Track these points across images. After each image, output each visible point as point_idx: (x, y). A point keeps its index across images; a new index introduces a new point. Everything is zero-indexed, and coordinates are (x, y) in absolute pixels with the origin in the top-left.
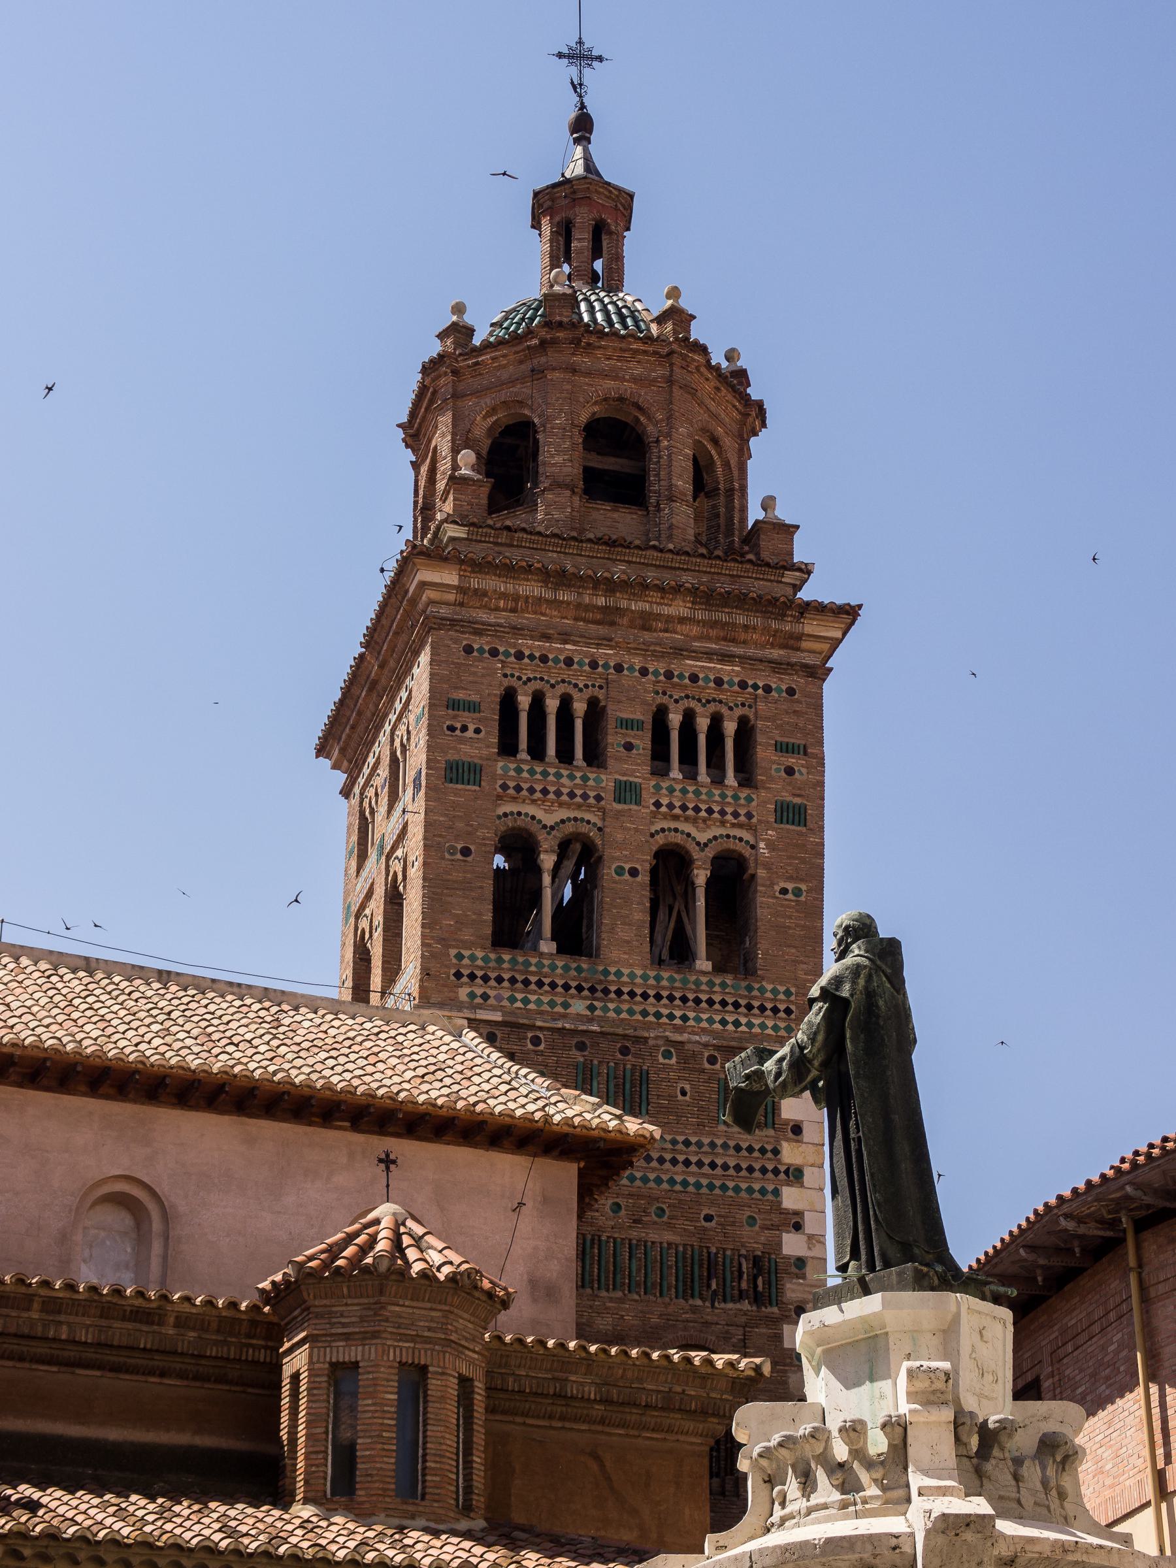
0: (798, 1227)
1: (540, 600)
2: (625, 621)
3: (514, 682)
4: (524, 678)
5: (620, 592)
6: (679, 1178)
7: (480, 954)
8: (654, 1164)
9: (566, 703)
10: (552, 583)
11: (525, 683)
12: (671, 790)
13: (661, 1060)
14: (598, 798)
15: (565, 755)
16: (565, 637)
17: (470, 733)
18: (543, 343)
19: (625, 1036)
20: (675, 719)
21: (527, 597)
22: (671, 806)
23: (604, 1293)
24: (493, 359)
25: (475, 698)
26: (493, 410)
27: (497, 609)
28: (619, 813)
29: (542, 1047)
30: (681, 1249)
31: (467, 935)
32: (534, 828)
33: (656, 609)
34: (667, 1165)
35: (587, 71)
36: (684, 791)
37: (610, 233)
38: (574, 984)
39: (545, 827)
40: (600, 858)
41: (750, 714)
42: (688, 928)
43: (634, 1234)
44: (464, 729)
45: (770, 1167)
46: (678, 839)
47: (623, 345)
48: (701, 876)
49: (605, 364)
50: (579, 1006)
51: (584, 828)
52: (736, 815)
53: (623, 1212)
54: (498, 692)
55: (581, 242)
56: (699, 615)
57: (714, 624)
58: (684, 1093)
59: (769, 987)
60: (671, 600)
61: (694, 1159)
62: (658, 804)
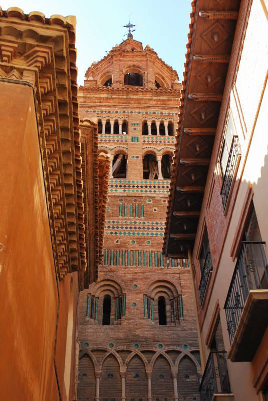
2: (133, 102)
3: (101, 118)
6: (155, 233)
8: (146, 229)
12: (148, 138)
13: (147, 202)
14: (126, 141)
16: (115, 107)
19: (135, 196)
20: (149, 123)
21: (104, 98)
26: (102, 77)
30: (156, 252)
34: (150, 230)
36: (152, 138)
38: (119, 185)
41: (172, 120)
42: (157, 174)
43: (140, 249)
46: (151, 149)
48: (159, 159)
49: (129, 59)
51: (122, 149)
52: (169, 142)
53: (135, 243)
56: (154, 98)
58: (155, 210)
61: (159, 228)
62: (144, 141)
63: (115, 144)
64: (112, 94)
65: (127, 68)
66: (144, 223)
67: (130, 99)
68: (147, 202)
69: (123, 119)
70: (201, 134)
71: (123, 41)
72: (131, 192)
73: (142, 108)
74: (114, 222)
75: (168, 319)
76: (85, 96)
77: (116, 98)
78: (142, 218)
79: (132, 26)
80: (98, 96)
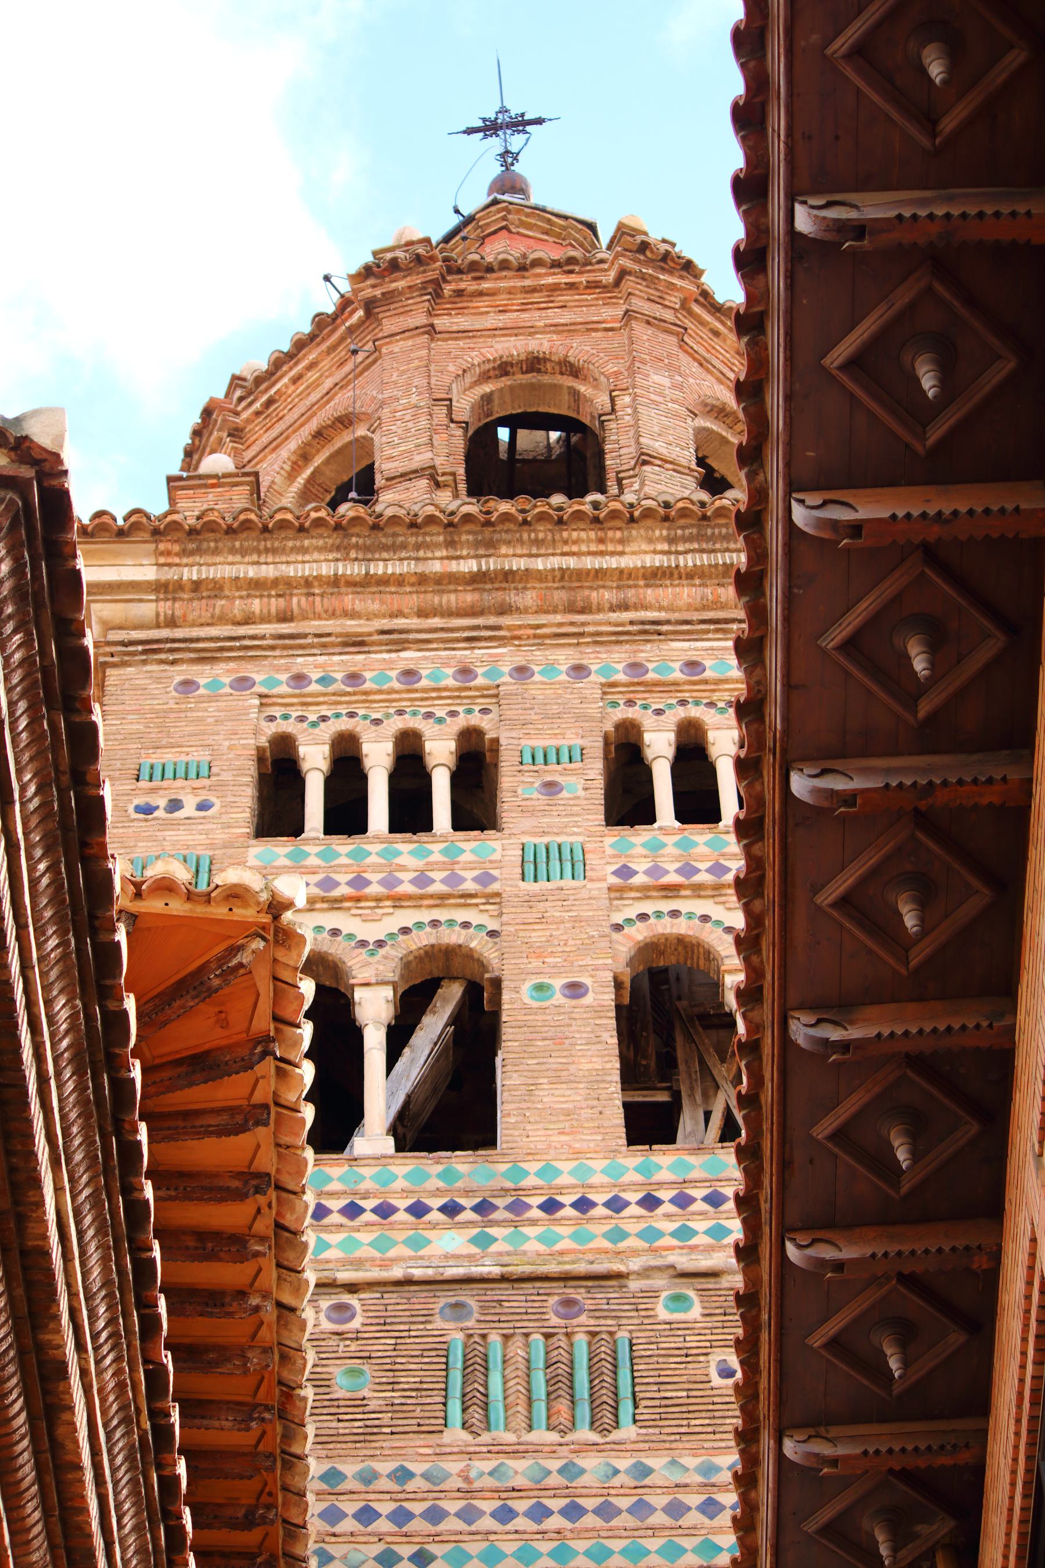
1: (335, 582)
2: (529, 598)
4: (313, 717)
5: (508, 543)
10: (357, 547)
11: (314, 725)
14: (485, 879)
17: (189, 809)
19: (566, 1278)
22: (655, 871)
24: (295, 380)
25: (201, 756)
26: (304, 456)
29: (356, 1324)
34: (694, 1518)
36: (685, 845)
39: (363, 943)
44: (175, 805)
46: (682, 927)
47: (527, 283)
51: (453, 937)
56: (689, 561)
60: (621, 541)
62: (625, 872)
63: (399, 901)
64: (369, 552)
65: (485, 377)
67: (508, 576)
68: (662, 1313)
69: (462, 721)
70: (934, 533)
71: (455, 220)
73: (598, 640)
74: (403, 1475)
76: (170, 575)
77: (400, 581)
78: (628, 1431)
79: (520, 124)
80: (268, 572)
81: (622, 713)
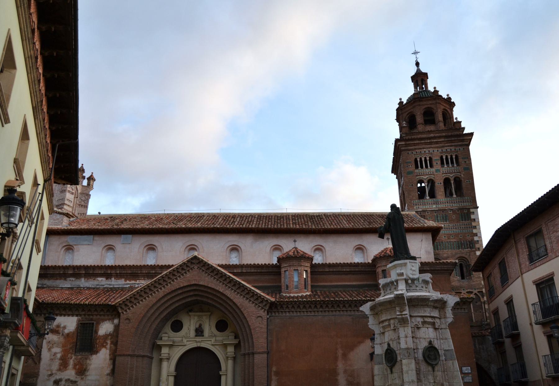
0: (477, 235)
2: (433, 143)
7: (417, 201)
9: (425, 158)
13: (449, 212)
14: (433, 173)
15: (427, 167)
16: (424, 148)
17: (410, 167)
18: (414, 102)
19: (443, 210)
22: (445, 172)
23: (445, 251)
25: (410, 161)
27: (412, 146)
28: (437, 175)
31: (414, 198)
32: (423, 179)
33: (438, 140)
35: (417, 55)
37: (424, 80)
40: (435, 182)
43: (449, 240)
44: (409, 166)
45: (470, 226)
46: (447, 177)
48: (452, 182)
50: (434, 206)
51: (431, 178)
54: (414, 159)
55: (420, 83)
56: (446, 140)
57: (448, 141)
58: (454, 217)
59: (466, 198)
62: (443, 172)
66: (449, 225)
67: (432, 142)
68: (449, 212)
72: (441, 206)
75: (465, 274)
78: (448, 222)
81: (441, 155)
